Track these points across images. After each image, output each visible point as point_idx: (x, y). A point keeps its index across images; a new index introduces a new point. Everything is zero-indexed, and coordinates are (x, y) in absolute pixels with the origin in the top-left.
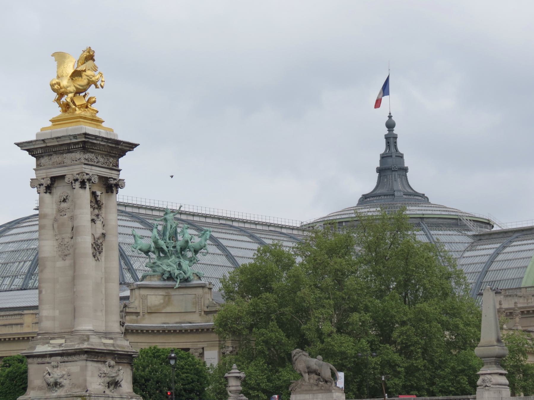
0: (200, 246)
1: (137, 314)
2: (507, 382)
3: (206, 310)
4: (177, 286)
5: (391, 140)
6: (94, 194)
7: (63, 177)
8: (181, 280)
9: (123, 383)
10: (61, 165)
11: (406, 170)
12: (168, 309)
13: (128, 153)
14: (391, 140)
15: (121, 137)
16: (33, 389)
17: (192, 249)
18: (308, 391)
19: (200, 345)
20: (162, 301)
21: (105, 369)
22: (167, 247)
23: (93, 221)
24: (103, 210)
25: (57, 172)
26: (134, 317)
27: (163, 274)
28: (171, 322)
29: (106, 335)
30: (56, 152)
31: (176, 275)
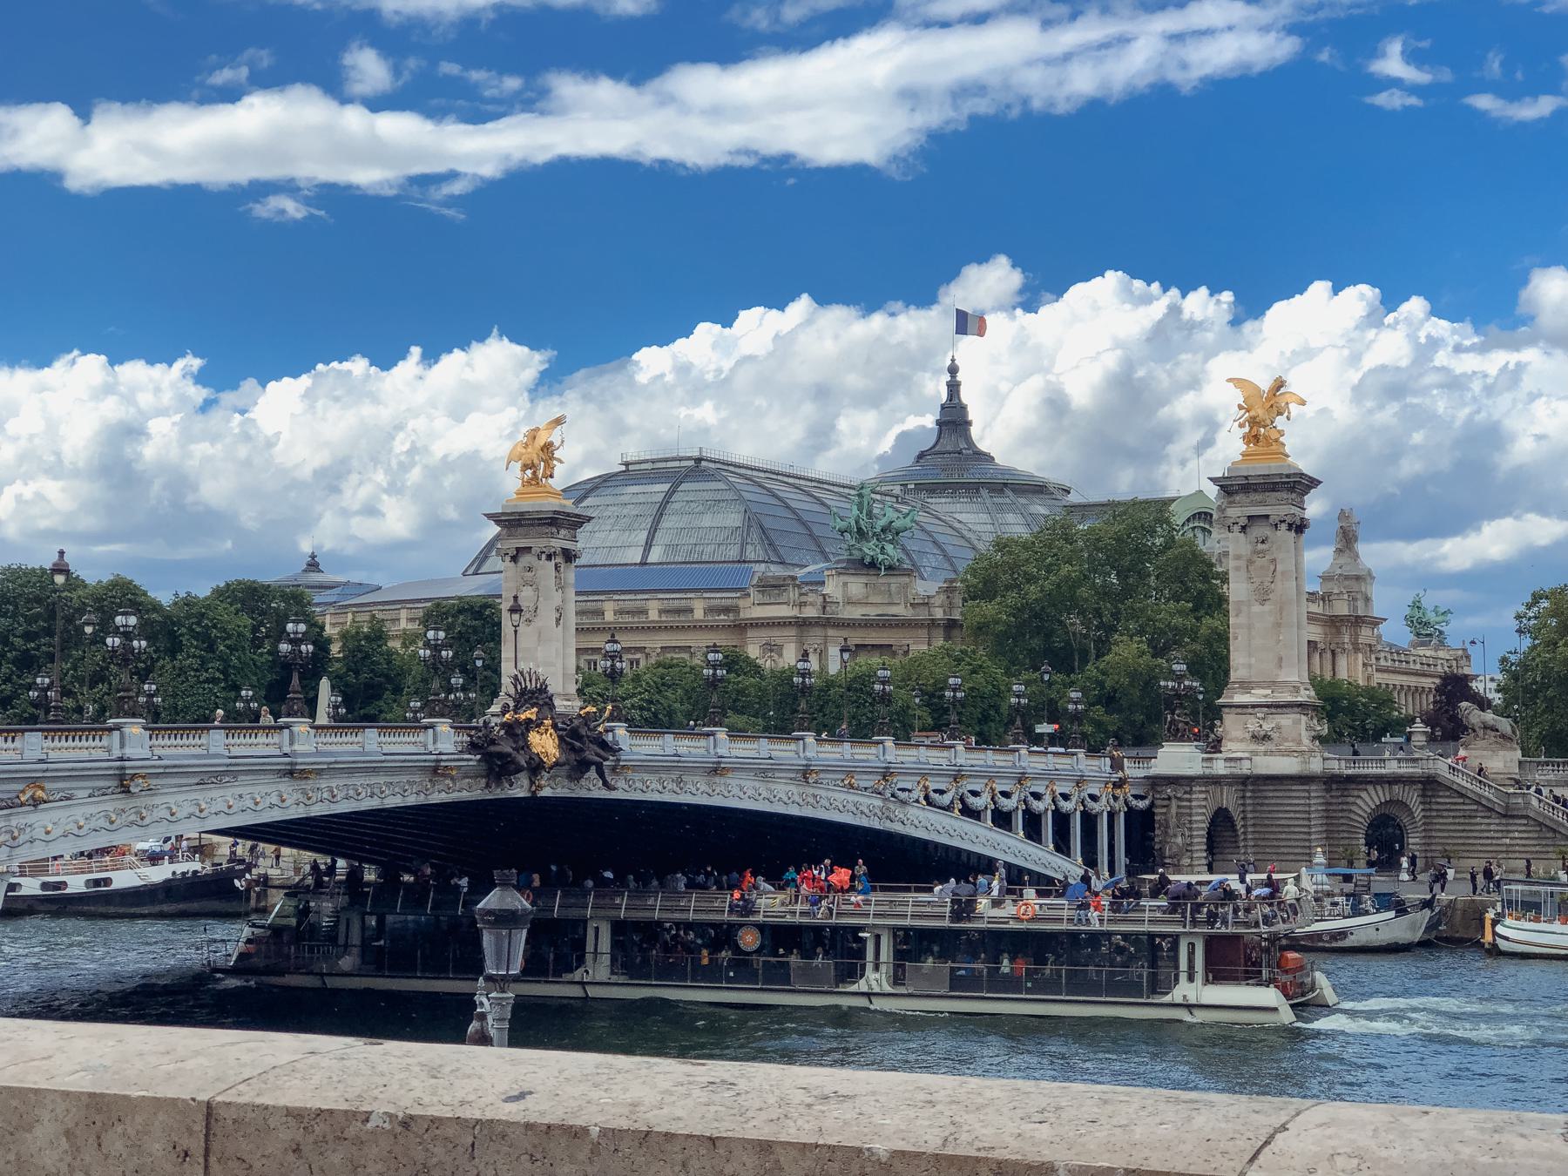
5: (954, 387)
7: (1267, 516)
10: (1262, 503)
11: (969, 423)
14: (954, 387)
30: (1255, 491)
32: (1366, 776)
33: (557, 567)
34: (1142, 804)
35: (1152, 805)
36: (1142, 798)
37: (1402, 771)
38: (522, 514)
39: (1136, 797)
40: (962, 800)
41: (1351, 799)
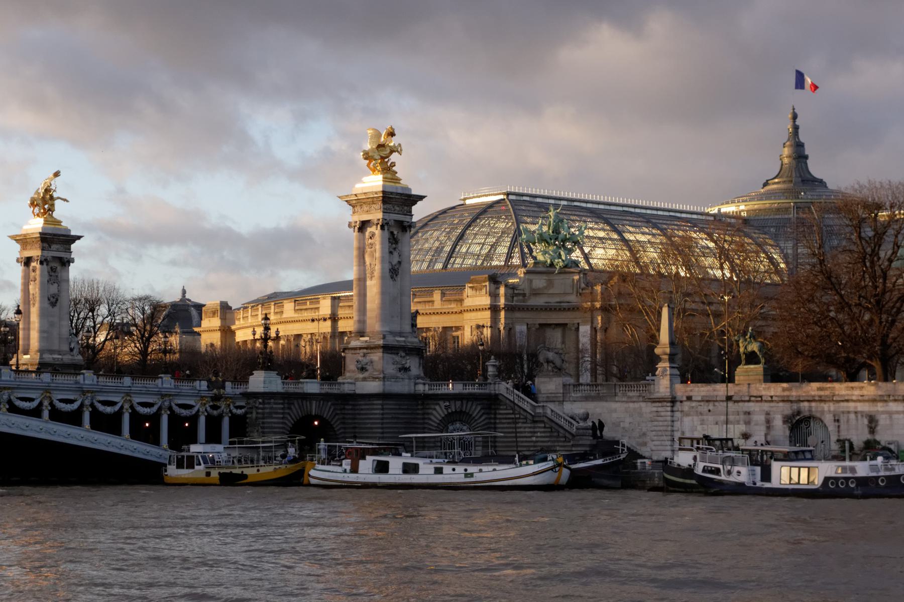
1: (524, 295)
2: (678, 373)
6: (392, 233)
9: (412, 368)
11: (806, 157)
12: (551, 292)
13: (419, 203)
15: (414, 192)
16: (349, 372)
18: (547, 376)
19: (576, 321)
21: (397, 358)
23: (391, 253)
24: (400, 244)
25: (365, 218)
26: (521, 298)
28: (554, 300)
29: (400, 334)
32: (438, 395)
33: (53, 270)
34: (239, 412)
35: (246, 413)
36: (241, 407)
37: (467, 391)
38: (25, 235)
39: (237, 407)
40: (10, 402)
41: (430, 411)
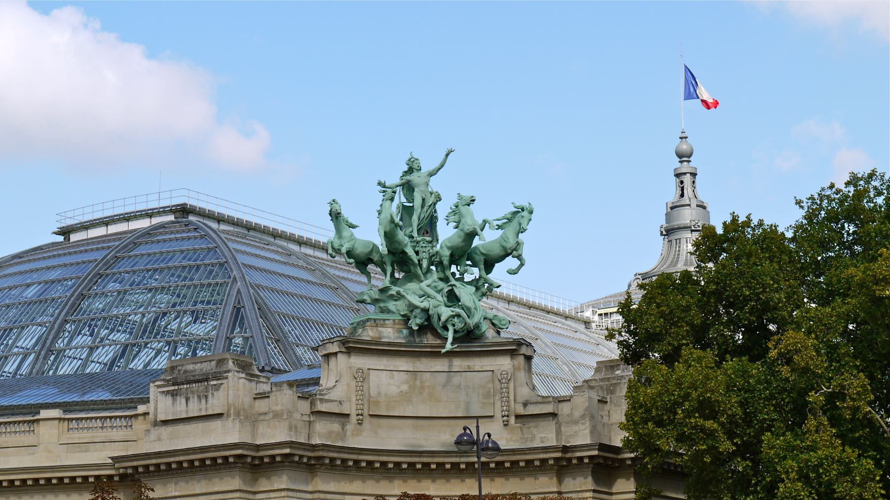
0: (504, 248)
3: (521, 410)
4: (448, 347)
8: (455, 332)
17: (480, 259)
20: (405, 387)
22: (417, 253)
27: (406, 319)
31: (443, 319)
